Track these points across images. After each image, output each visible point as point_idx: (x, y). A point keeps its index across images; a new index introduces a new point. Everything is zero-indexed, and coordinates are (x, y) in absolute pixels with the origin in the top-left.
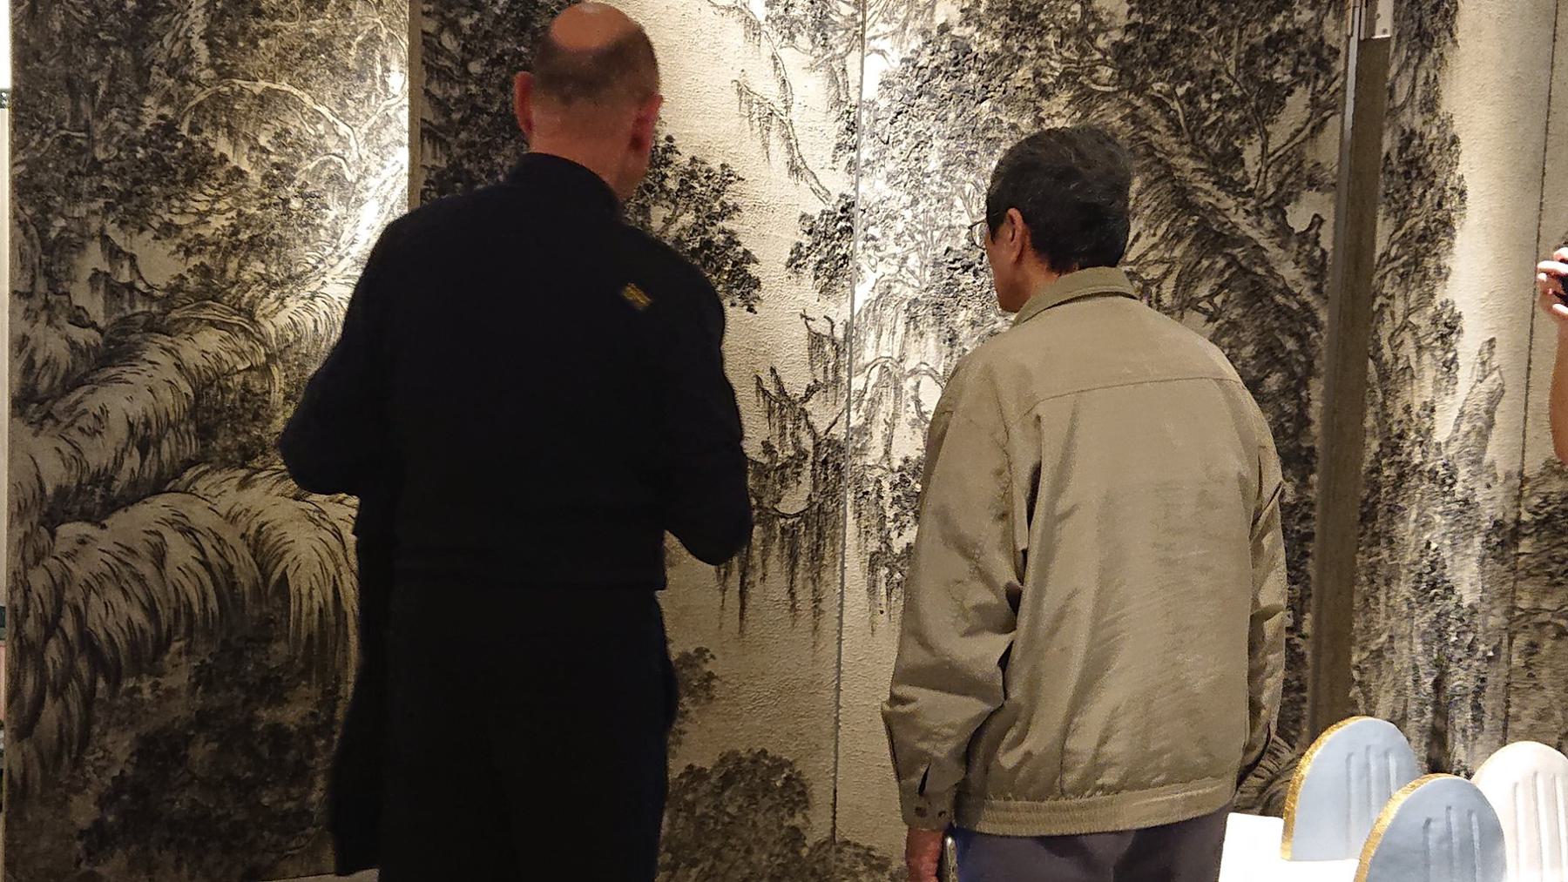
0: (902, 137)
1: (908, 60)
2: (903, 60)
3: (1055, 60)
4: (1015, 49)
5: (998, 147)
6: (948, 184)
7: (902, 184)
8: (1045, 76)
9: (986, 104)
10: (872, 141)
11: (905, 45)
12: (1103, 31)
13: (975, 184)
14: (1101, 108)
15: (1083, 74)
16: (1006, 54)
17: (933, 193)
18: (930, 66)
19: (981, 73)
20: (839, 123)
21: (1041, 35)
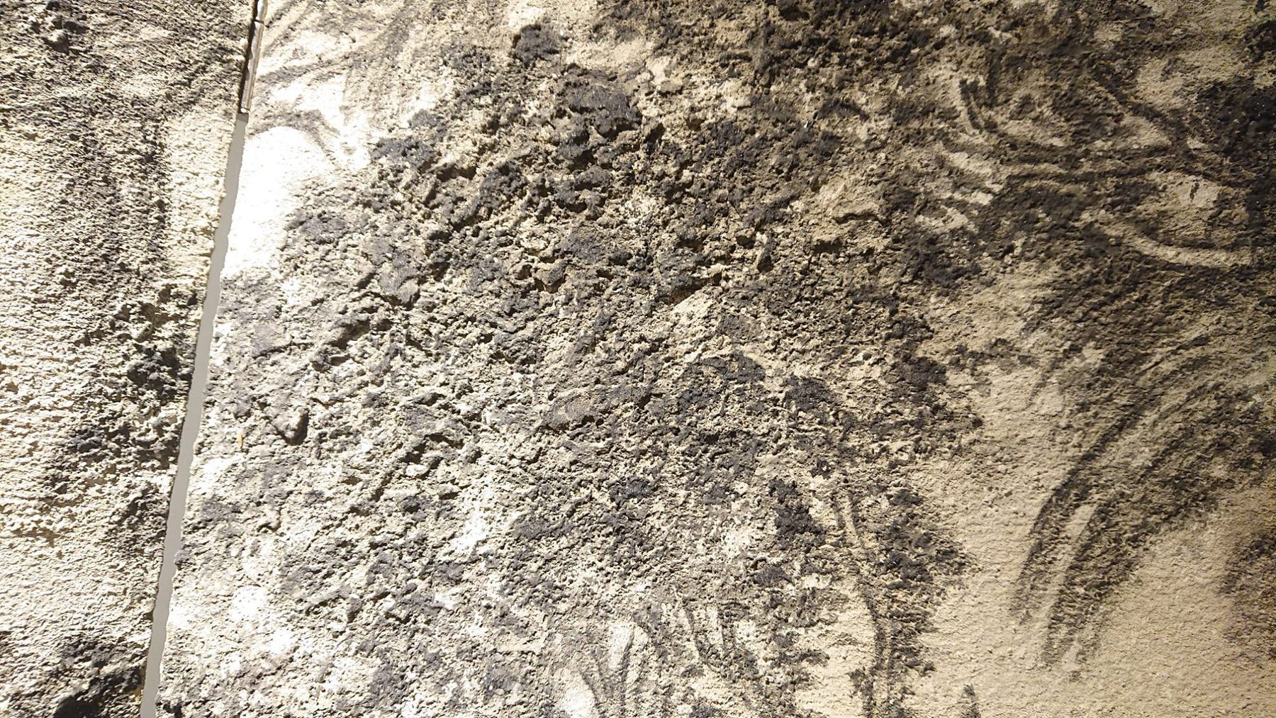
0: (356, 414)
1: (408, 148)
2: (381, 148)
3: (969, 149)
4: (806, 113)
5: (745, 470)
6: (536, 615)
7: (342, 610)
8: (930, 206)
9: (697, 304)
10: (239, 430)
11: (393, 100)
12: (1158, 50)
13: (650, 621)
14: (1191, 334)
15: (1092, 201)
16: (766, 128)
17: (471, 652)
18: (483, 168)
19: (673, 193)
20: (96, 352)
21: (903, 61)
